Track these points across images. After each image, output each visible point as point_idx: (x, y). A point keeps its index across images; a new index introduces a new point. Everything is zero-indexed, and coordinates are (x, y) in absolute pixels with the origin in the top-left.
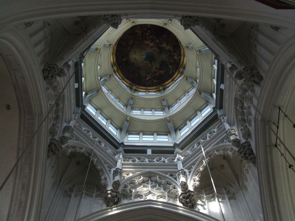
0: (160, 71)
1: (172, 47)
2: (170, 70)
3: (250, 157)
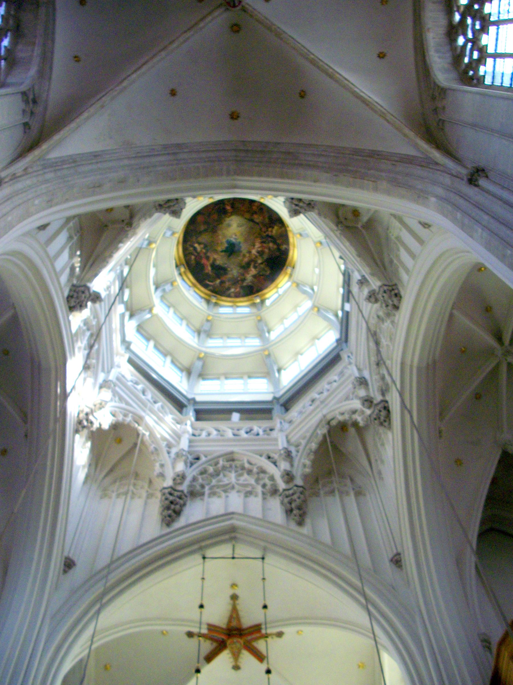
1: (250, 284)
2: (212, 282)
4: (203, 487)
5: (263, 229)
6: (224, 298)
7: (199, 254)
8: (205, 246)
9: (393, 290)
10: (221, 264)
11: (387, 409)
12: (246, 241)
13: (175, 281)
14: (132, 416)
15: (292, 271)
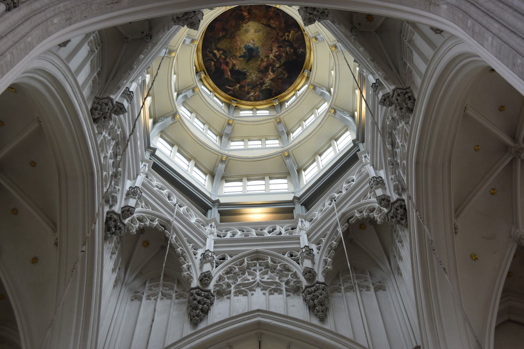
0: (230, 71)
2: (232, 87)
3: (201, 313)
4: (229, 286)
5: (280, 34)
6: (243, 102)
7: (218, 59)
8: (224, 52)
9: (407, 93)
10: (240, 69)
11: (403, 207)
12: (263, 45)
13: (197, 87)
14: (158, 220)
15: (309, 74)
